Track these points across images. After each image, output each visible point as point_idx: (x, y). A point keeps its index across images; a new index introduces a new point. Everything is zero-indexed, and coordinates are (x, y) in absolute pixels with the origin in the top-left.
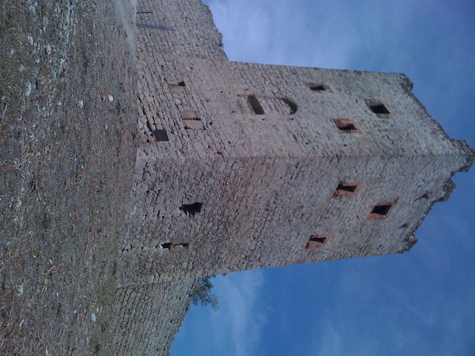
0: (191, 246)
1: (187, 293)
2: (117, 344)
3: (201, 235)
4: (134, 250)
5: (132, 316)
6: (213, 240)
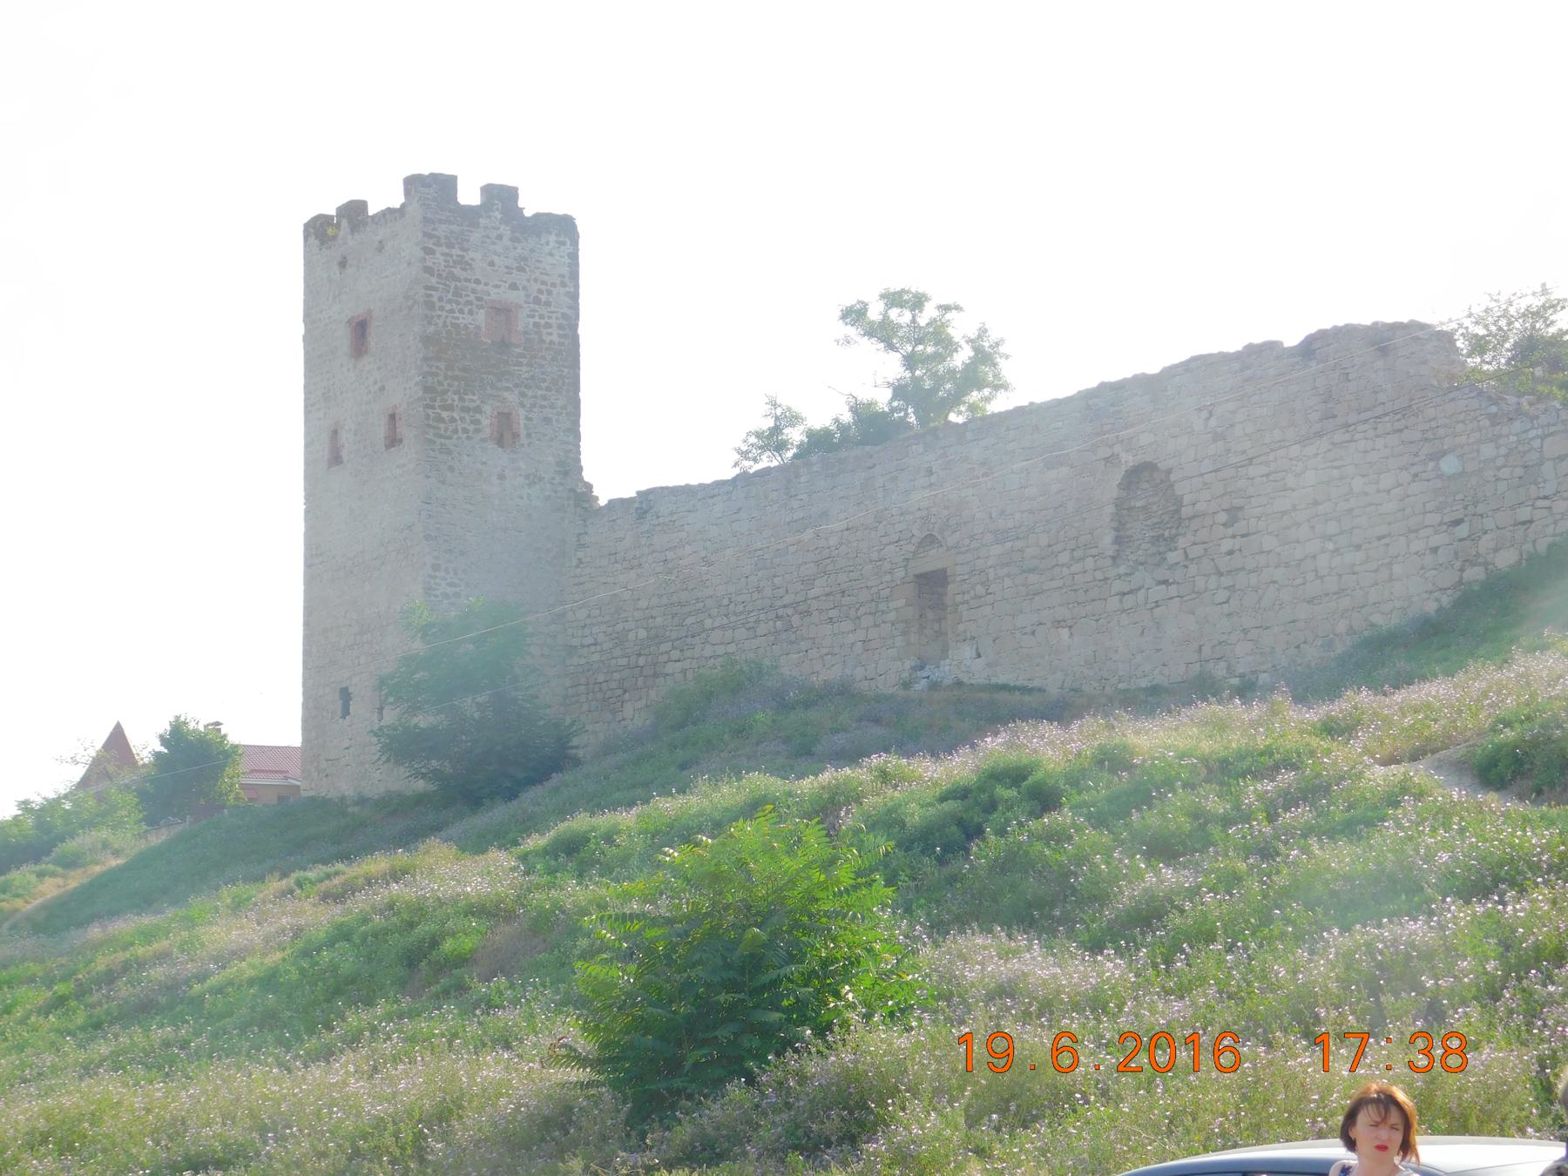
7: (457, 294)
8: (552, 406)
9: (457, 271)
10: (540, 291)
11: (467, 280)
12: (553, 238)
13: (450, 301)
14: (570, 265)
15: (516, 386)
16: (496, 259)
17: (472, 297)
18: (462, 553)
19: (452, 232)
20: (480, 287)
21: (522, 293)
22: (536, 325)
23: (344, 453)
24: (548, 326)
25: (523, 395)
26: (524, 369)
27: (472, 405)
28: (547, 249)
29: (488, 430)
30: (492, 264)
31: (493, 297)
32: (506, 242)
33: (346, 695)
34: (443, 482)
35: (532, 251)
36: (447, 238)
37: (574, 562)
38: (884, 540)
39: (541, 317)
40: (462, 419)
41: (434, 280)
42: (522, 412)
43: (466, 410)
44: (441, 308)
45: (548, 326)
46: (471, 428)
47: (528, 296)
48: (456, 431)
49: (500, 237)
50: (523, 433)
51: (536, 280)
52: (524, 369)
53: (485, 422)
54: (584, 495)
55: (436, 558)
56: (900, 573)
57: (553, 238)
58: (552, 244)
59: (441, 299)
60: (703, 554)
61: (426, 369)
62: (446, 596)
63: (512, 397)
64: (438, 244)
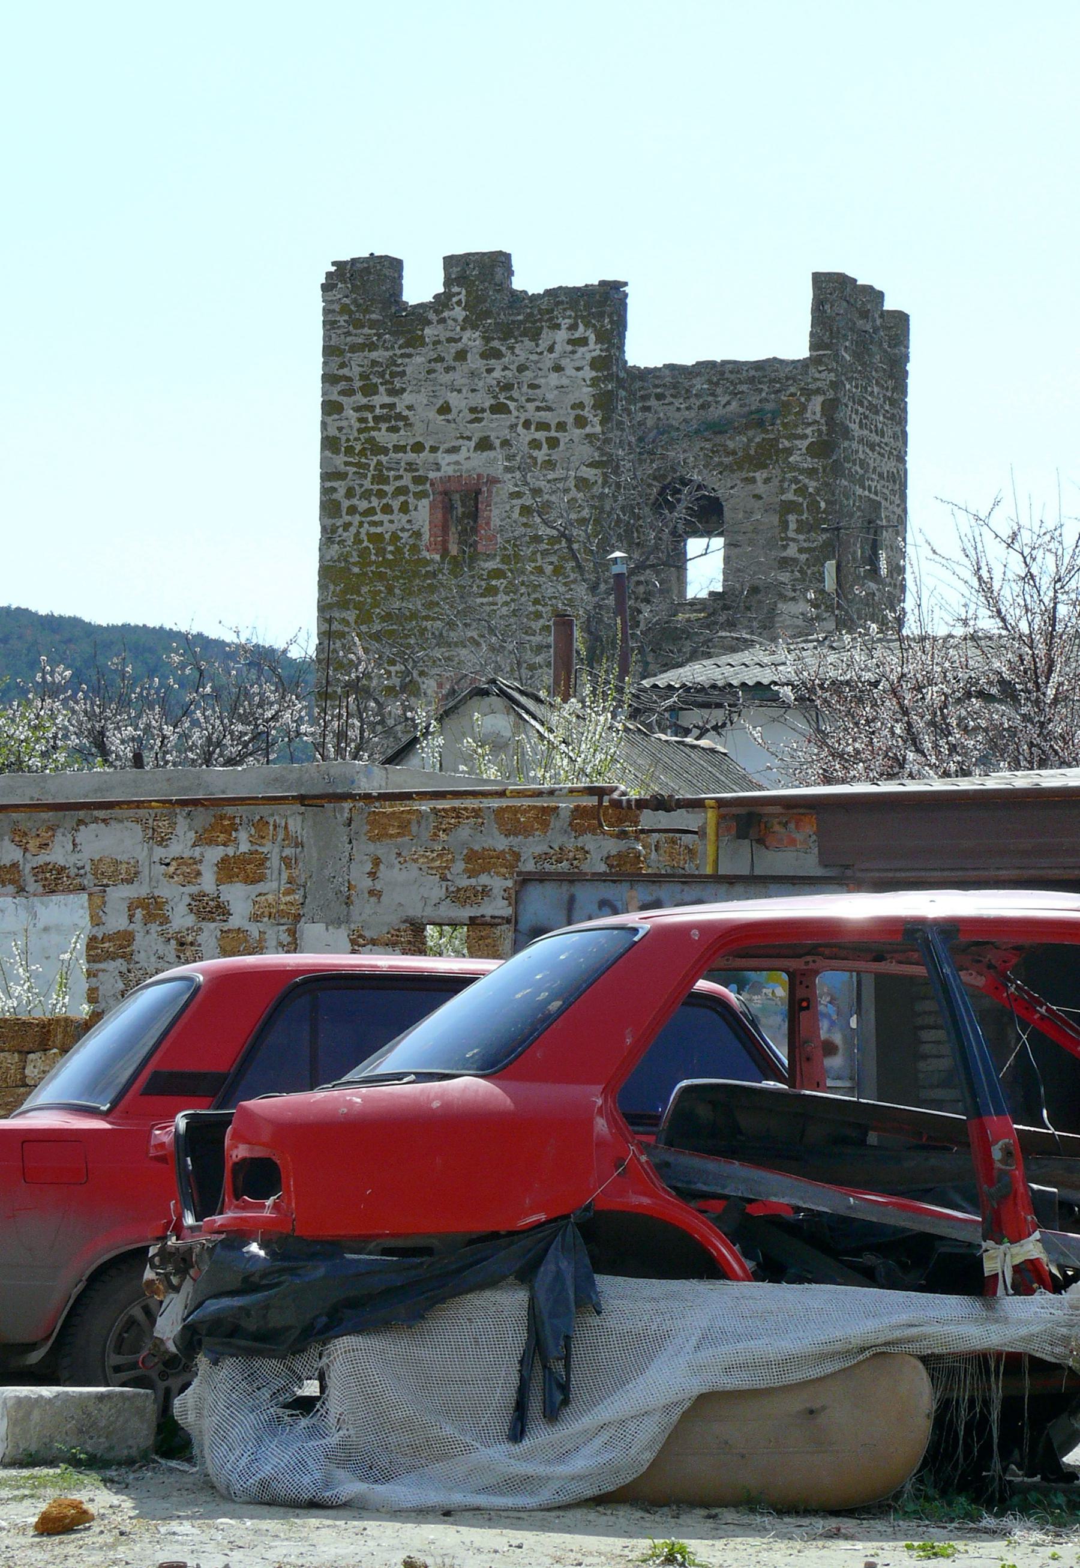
7: (380, 478)
9: (383, 436)
10: (535, 444)
12: (562, 335)
13: (366, 495)
14: (595, 382)
16: (453, 399)
17: (407, 480)
19: (374, 363)
22: (526, 510)
26: (501, 598)
30: (445, 409)
31: (447, 470)
32: (474, 362)
35: (521, 369)
36: (364, 376)
41: (340, 460)
44: (352, 510)
49: (461, 355)
51: (527, 424)
57: (562, 335)
59: (350, 493)
64: (348, 392)
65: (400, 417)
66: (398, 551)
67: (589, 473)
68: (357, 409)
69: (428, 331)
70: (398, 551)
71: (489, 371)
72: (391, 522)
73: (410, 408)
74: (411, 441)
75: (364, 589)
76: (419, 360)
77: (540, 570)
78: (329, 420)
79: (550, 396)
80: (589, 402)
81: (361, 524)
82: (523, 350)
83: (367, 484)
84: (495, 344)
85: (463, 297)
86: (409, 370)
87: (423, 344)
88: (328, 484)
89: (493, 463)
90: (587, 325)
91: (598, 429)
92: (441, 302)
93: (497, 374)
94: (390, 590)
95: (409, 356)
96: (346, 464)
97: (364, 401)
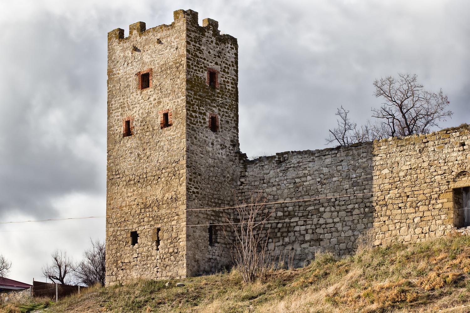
0: (159, 226)
1: (335, 157)
2: (400, 208)
3: (152, 223)
4: (158, 265)
5: (357, 206)
6: (157, 210)
7: (198, 63)
8: (229, 116)
9: (197, 53)
10: (225, 67)
11: (201, 58)
13: (195, 66)
15: (217, 106)
16: (211, 51)
17: (203, 66)
18: (200, 175)
19: (196, 36)
20: (205, 62)
21: (220, 67)
22: (224, 81)
23: (134, 131)
24: (228, 82)
25: (219, 110)
27: (203, 112)
28: (227, 50)
29: (208, 124)
30: (209, 53)
31: (210, 67)
32: (214, 44)
33: (135, 236)
34: (193, 143)
35: (223, 49)
37: (239, 183)
38: (435, 174)
39: (226, 78)
40: (199, 117)
42: (219, 117)
43: (200, 113)
45: (228, 82)
46: (203, 121)
47: (221, 68)
48: (197, 122)
49: (212, 42)
50: (220, 126)
51: (224, 62)
52: (220, 99)
53: (207, 120)
54: (243, 156)
55: (190, 176)
56: (444, 187)
58: (229, 48)
59: (192, 64)
60: (319, 180)
61: (187, 94)
62: (194, 192)
63: (216, 110)
64: (192, 41)
65: (201, 50)
66: (201, 81)
67: (235, 78)
68: (193, 45)
69: (206, 33)
70: (201, 81)
71: (217, 48)
72: (200, 74)
73: (203, 49)
74: (203, 57)
75: (195, 88)
76: (204, 39)
77: (226, 95)
78: (188, 45)
79: (228, 58)
80: (234, 62)
81: (194, 72)
82: (223, 45)
83: (195, 64)
84: (218, 42)
85: (212, 29)
86: (203, 41)
87: (205, 36)
88: (188, 61)
89: (217, 68)
90: (234, 45)
91: (236, 69)
92: (208, 28)
93: (218, 49)
94: (200, 90)
95: (203, 38)
96: (191, 57)
97: (195, 44)
